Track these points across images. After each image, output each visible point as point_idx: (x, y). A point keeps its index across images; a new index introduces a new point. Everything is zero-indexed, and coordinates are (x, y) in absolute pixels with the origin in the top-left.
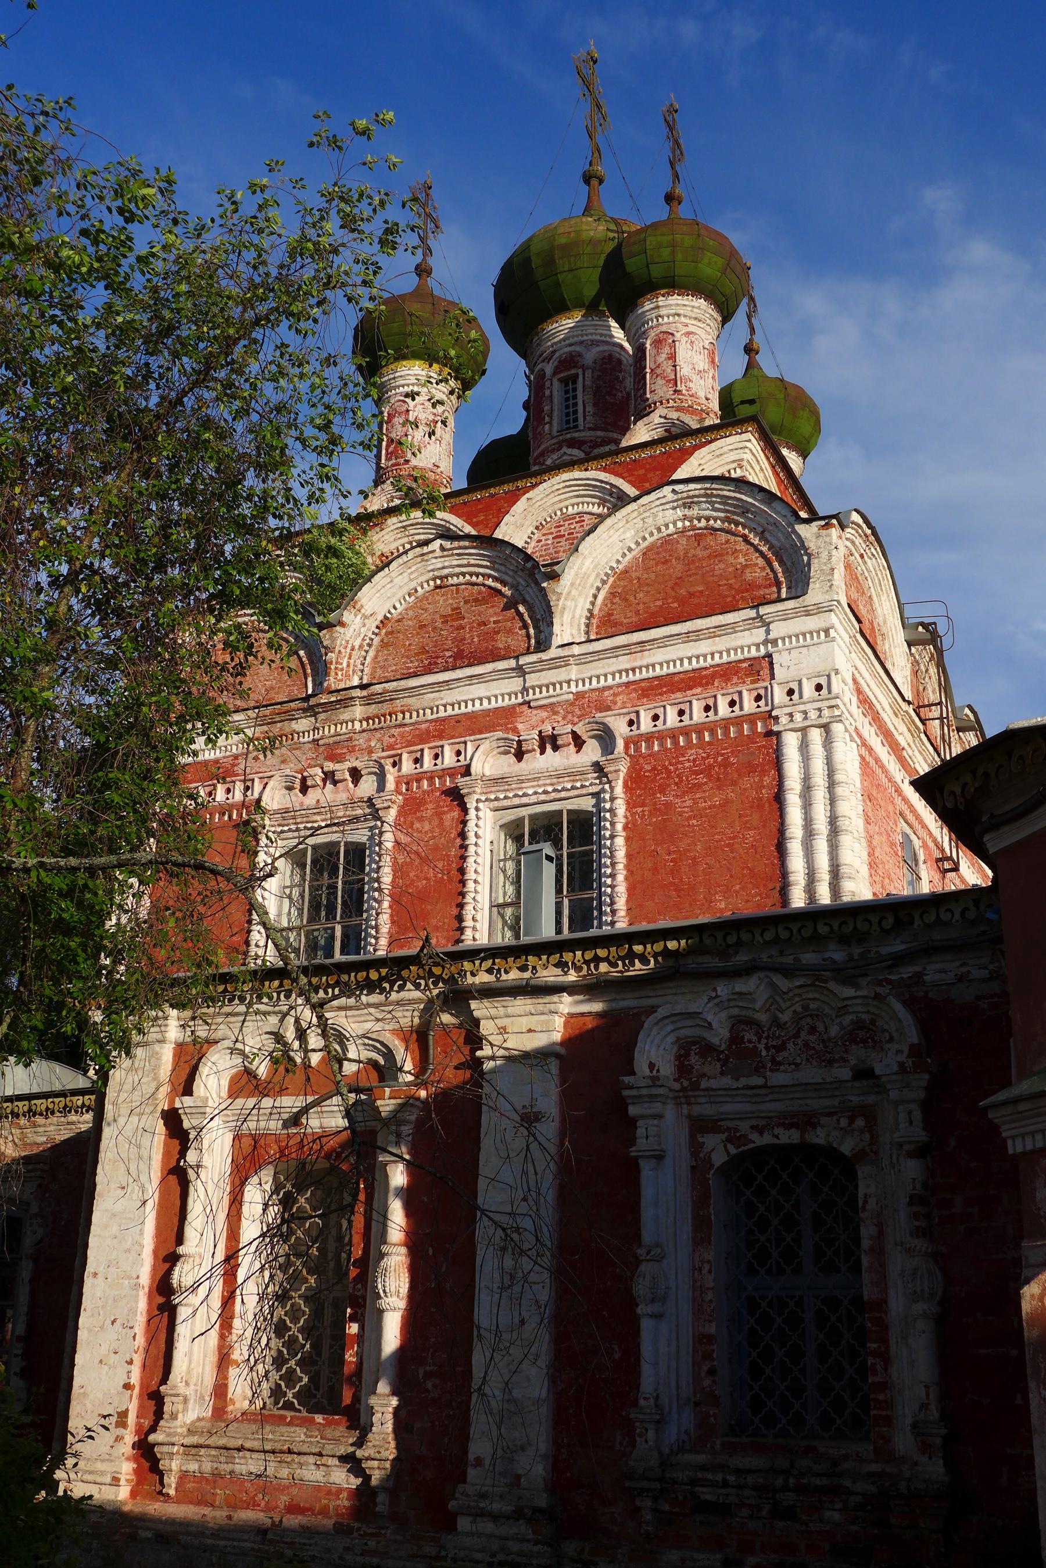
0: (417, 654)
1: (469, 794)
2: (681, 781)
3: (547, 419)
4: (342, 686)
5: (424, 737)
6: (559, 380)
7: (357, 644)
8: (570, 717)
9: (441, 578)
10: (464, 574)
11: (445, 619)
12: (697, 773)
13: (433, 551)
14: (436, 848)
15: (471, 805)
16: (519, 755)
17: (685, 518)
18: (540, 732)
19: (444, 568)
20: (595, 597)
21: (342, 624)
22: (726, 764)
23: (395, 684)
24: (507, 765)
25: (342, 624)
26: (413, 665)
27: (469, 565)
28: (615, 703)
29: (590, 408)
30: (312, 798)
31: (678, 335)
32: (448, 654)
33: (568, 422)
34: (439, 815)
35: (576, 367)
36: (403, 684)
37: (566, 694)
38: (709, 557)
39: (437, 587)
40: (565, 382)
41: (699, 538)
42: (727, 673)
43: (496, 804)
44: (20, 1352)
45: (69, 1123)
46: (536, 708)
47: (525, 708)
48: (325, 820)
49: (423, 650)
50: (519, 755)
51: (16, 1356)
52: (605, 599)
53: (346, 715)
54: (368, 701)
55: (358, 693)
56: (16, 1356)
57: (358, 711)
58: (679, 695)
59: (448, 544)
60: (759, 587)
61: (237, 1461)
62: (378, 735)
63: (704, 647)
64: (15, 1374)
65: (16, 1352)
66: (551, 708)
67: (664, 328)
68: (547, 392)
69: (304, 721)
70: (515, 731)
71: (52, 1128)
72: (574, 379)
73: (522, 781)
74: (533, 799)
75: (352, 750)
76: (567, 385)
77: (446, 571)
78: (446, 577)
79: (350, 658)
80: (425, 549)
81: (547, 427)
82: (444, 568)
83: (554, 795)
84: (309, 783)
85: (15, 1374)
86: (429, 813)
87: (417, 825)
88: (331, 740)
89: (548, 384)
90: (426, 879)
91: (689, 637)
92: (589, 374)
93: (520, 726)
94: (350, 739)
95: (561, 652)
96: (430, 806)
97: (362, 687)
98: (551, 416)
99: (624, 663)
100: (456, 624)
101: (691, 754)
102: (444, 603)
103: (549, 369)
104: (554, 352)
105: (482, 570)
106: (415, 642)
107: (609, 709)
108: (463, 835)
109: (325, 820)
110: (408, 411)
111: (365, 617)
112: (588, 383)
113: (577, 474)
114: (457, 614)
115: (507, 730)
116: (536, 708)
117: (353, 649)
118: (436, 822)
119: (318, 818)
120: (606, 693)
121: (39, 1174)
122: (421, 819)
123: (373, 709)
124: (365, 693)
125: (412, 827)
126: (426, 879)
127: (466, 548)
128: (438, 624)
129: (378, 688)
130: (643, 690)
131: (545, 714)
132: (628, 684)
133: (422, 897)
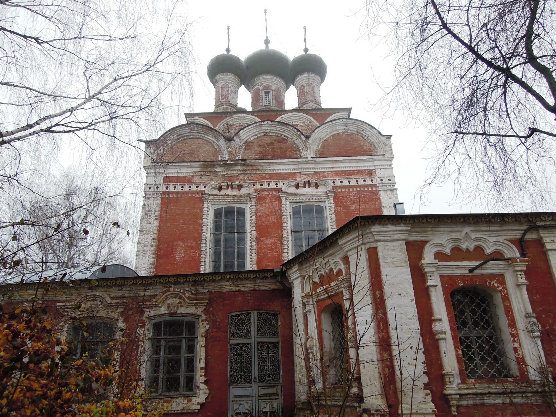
0: (258, 154)
1: (282, 197)
2: (351, 200)
3: (261, 101)
4: (233, 159)
5: (264, 178)
6: (264, 92)
7: (237, 147)
8: (314, 178)
9: (266, 133)
10: (273, 133)
11: (268, 145)
12: (356, 199)
13: (265, 124)
14: (271, 212)
15: (283, 200)
16: (297, 186)
17: (345, 129)
18: (305, 181)
19: (268, 130)
20: (318, 146)
21: (234, 141)
22: (364, 197)
23: (254, 161)
24: (293, 190)
25: (234, 141)
26: (257, 157)
27: (276, 130)
28: (328, 176)
29: (274, 101)
30: (223, 192)
31: (314, 85)
32: (270, 155)
33: (267, 103)
34: (272, 202)
35: (270, 89)
36: (257, 161)
37: (312, 171)
38: (353, 141)
39: (265, 135)
40: (266, 92)
41: (349, 135)
42: (362, 172)
43: (291, 201)
44: (203, 374)
45: (220, 285)
46: (302, 174)
47: (299, 174)
48: (230, 200)
49: (260, 153)
50: (297, 186)
51: (201, 376)
52: (321, 147)
53: (236, 168)
54: (244, 165)
55: (240, 162)
56: (201, 376)
57: (239, 168)
58: (348, 176)
59: (270, 123)
60: (368, 151)
61: (485, 398)
62: (247, 176)
63: (355, 164)
64: (202, 383)
65: (201, 374)
66: (308, 175)
67: (310, 82)
68: (261, 94)
69: (219, 168)
70: (296, 180)
71: (211, 287)
72: (269, 92)
73: (301, 195)
74: (304, 200)
75: (238, 179)
76: (266, 93)
77: (268, 131)
78: (268, 132)
79: (236, 151)
80: (263, 123)
81: (261, 104)
82: (268, 130)
83: (311, 200)
84: (222, 187)
85: (202, 383)
86: (268, 201)
87: (264, 204)
88: (229, 175)
89: (261, 92)
90: (269, 221)
91: (350, 161)
92: (273, 91)
93: (297, 179)
94: (237, 176)
95: (312, 159)
96: (268, 199)
97: (242, 160)
98: (262, 100)
99: (330, 165)
100: (272, 147)
101: (354, 193)
102: (267, 140)
103: (261, 88)
104: (262, 84)
105: (280, 132)
106: (258, 150)
107: (326, 177)
108: (280, 209)
109: (230, 200)
110: (229, 88)
111: (240, 139)
112: (274, 94)
113: (297, 113)
114: (271, 144)
115: (293, 179)
116: (302, 174)
117: (236, 148)
118: (271, 204)
119: (228, 199)
120: (325, 173)
121: (206, 304)
122: (265, 203)
123: (244, 168)
124: (243, 162)
125: (262, 204)
126: (269, 221)
127: (276, 125)
128: (266, 146)
129: (248, 161)
130: (337, 174)
131: (306, 177)
132: (331, 171)
133: (268, 226)
